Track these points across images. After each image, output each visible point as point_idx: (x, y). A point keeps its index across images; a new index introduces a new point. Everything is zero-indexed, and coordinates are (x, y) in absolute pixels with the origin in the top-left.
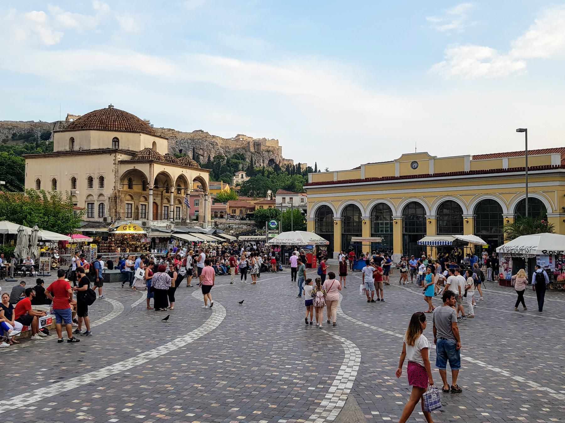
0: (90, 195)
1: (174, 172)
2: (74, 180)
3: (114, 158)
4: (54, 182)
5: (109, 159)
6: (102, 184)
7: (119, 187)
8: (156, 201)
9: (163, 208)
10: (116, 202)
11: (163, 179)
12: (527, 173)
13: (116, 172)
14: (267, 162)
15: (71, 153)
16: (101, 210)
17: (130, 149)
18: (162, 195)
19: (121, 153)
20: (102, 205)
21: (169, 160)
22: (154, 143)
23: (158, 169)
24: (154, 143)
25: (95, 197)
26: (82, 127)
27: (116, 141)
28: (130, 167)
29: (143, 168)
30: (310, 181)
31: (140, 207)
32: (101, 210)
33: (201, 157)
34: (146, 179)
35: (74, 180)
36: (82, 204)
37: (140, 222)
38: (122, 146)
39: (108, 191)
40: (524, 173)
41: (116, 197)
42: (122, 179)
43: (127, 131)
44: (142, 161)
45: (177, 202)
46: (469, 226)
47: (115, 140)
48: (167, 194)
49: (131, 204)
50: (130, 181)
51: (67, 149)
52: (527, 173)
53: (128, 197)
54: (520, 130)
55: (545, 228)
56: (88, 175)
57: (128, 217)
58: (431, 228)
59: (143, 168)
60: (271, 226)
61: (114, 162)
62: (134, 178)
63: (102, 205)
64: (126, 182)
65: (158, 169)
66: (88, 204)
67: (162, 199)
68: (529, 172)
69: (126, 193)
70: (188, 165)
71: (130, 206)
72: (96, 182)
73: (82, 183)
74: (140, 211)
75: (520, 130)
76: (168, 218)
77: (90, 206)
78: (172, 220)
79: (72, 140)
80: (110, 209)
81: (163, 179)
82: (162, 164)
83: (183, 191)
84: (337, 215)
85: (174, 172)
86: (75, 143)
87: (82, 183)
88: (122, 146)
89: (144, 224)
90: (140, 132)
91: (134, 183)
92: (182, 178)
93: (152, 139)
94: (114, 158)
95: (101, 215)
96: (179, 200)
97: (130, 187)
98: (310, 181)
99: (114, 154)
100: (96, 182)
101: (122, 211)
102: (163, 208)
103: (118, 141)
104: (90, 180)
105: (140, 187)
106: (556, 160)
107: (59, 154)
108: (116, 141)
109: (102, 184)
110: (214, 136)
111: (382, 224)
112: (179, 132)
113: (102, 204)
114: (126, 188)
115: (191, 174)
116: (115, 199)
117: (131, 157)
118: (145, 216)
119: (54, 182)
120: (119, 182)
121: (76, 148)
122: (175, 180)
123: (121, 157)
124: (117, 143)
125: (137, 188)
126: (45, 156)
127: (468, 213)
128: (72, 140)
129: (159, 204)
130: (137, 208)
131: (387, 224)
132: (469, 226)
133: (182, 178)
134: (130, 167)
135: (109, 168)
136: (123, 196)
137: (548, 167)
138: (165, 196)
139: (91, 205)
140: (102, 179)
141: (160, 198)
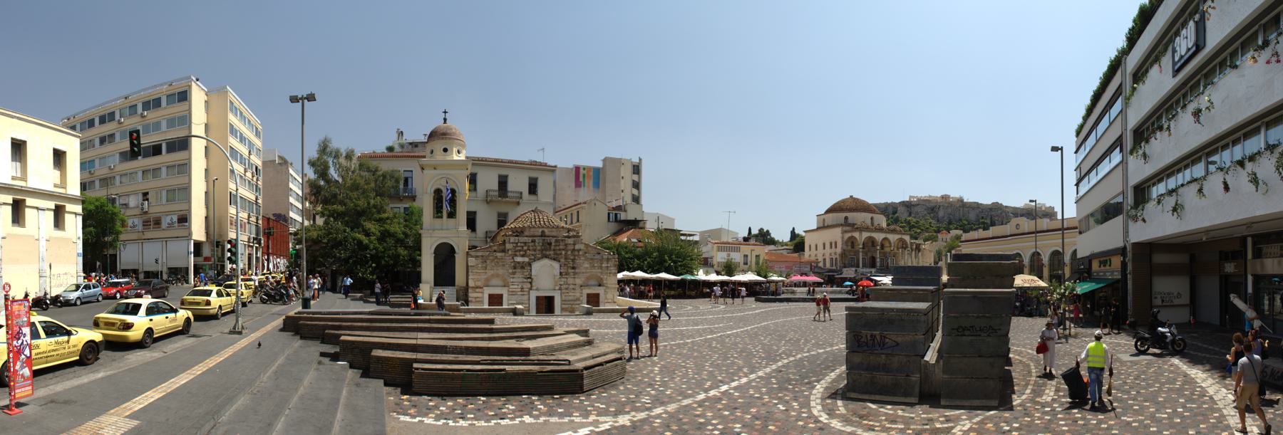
1: (879, 237)
5: (838, 231)
11: (872, 242)
21: (880, 230)
23: (865, 235)
27: (846, 218)
29: (856, 235)
36: (820, 259)
38: (850, 221)
39: (839, 250)
59: (856, 235)
62: (852, 242)
65: (865, 235)
87: (828, 245)
93: (870, 215)
108: (846, 218)
116: (843, 255)
133: (885, 239)
135: (836, 235)
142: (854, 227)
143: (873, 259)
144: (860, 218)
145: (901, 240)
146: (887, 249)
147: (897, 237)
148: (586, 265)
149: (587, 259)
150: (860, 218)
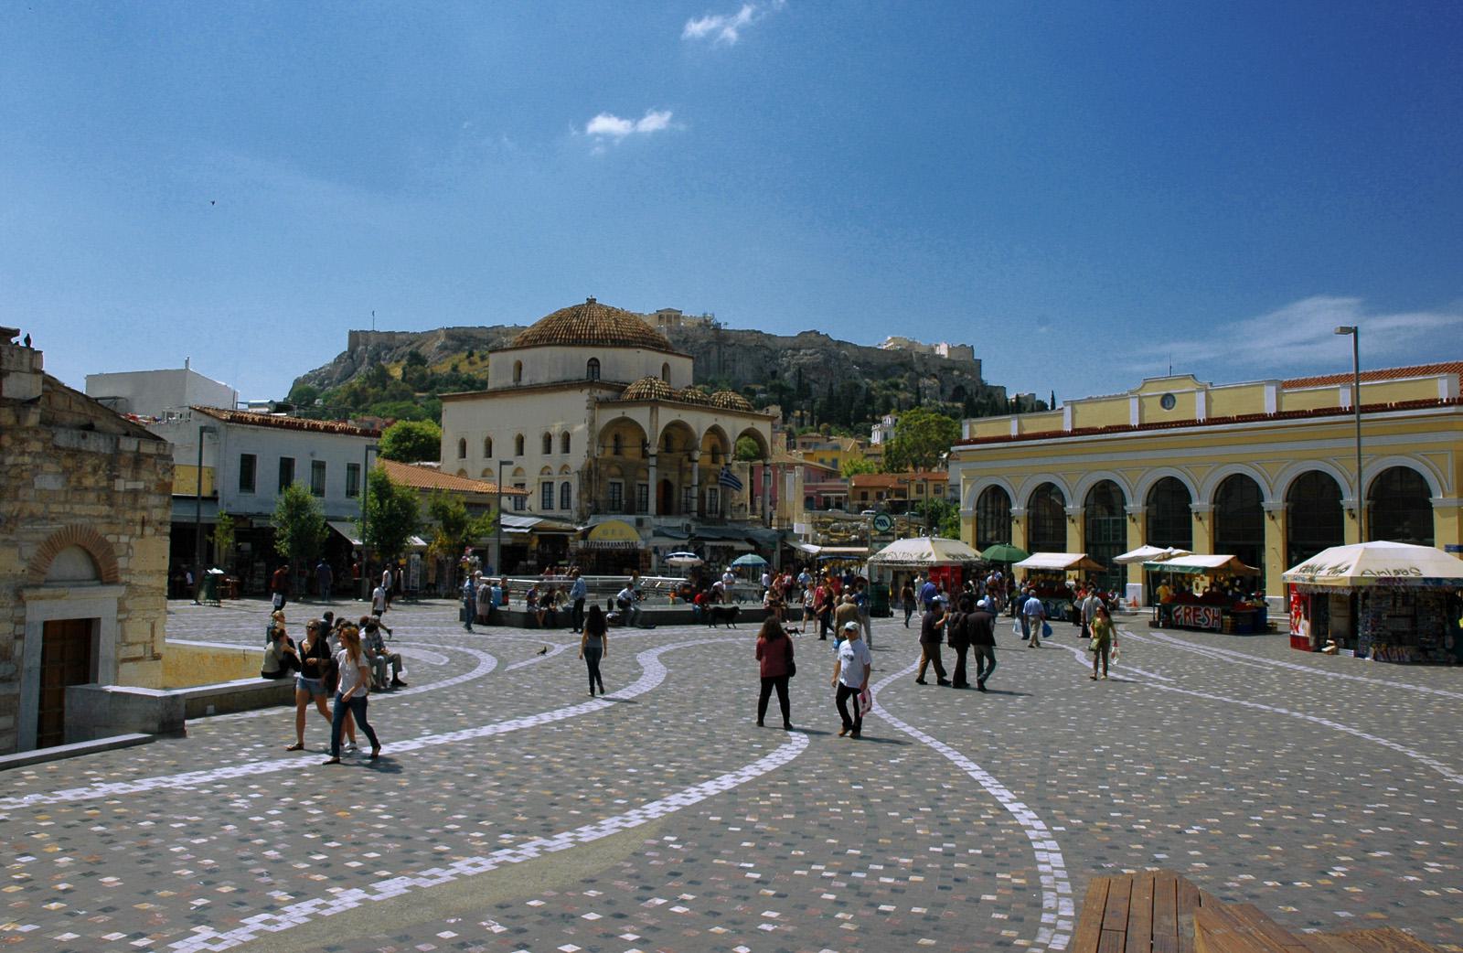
0: (547, 467)
1: (699, 422)
2: (520, 442)
3: (587, 397)
4: (489, 445)
5: (578, 400)
6: (566, 448)
7: (597, 452)
8: (670, 478)
9: (684, 491)
10: (590, 480)
11: (676, 436)
12: (1358, 417)
13: (592, 422)
14: (949, 392)
15: (517, 390)
16: (565, 496)
17: (622, 377)
18: (680, 465)
19: (598, 387)
20: (566, 487)
22: (666, 368)
23: (667, 416)
24: (666, 368)
25: (555, 470)
26: (536, 341)
27: (594, 363)
28: (615, 413)
29: (640, 415)
30: (966, 437)
31: (637, 490)
32: (565, 496)
33: (814, 386)
34: (645, 434)
35: (520, 442)
37: (632, 518)
39: (578, 458)
40: (1353, 417)
41: (590, 470)
42: (602, 436)
44: (639, 400)
45: (712, 478)
46: (1201, 531)
47: (593, 362)
48: (690, 465)
49: (620, 484)
50: (617, 438)
51: (510, 382)
52: (1358, 417)
53: (614, 470)
54: (1345, 331)
55: (1423, 535)
56: (543, 431)
57: (613, 509)
58: (1134, 531)
59: (640, 415)
60: (878, 527)
61: (586, 404)
63: (566, 487)
64: (610, 442)
65: (667, 416)
66: (544, 483)
67: (680, 474)
68: (1364, 416)
69: (610, 463)
70: (730, 409)
71: (617, 487)
72: (556, 444)
73: (534, 444)
74: (637, 496)
75: (1345, 331)
76: (688, 511)
77: (547, 487)
78: (695, 514)
79: (519, 366)
80: (580, 494)
81: (676, 436)
82: (674, 406)
83: (722, 458)
84: (1018, 508)
85: (699, 422)
86: (523, 371)
87: (534, 444)
88: (606, 373)
89: (639, 523)
90: (636, 347)
91: (627, 443)
92: (715, 430)
93: (659, 358)
94: (587, 397)
95: (565, 504)
96: (717, 477)
97: (617, 452)
98: (966, 437)
99: (587, 391)
100: (556, 444)
101: (601, 497)
102: (684, 491)
103: (598, 366)
104: (548, 440)
105: (638, 450)
106: (1442, 387)
107: (496, 393)
108: (594, 363)
109: (566, 448)
110: (840, 343)
111: (1106, 522)
112: (769, 337)
113: (567, 483)
114: (609, 453)
115: (733, 426)
116: (590, 475)
117: (615, 393)
118: (644, 509)
119: (489, 445)
121: (525, 381)
122: (702, 436)
123: (605, 394)
124: (596, 368)
125: (632, 453)
126: (473, 397)
127: (1201, 503)
128: (519, 366)
129: (675, 482)
130: (631, 491)
131: (1115, 522)
132: (1201, 531)
133: (715, 430)
134: (615, 413)
136: (603, 468)
137: (1432, 403)
138: (686, 468)
139: (547, 487)
140: (566, 438)
141: (676, 473)
142: (617, 392)
144: (633, 365)
145: (749, 433)
147: (744, 424)
148: (49, 480)
149: (54, 451)
150: (633, 365)
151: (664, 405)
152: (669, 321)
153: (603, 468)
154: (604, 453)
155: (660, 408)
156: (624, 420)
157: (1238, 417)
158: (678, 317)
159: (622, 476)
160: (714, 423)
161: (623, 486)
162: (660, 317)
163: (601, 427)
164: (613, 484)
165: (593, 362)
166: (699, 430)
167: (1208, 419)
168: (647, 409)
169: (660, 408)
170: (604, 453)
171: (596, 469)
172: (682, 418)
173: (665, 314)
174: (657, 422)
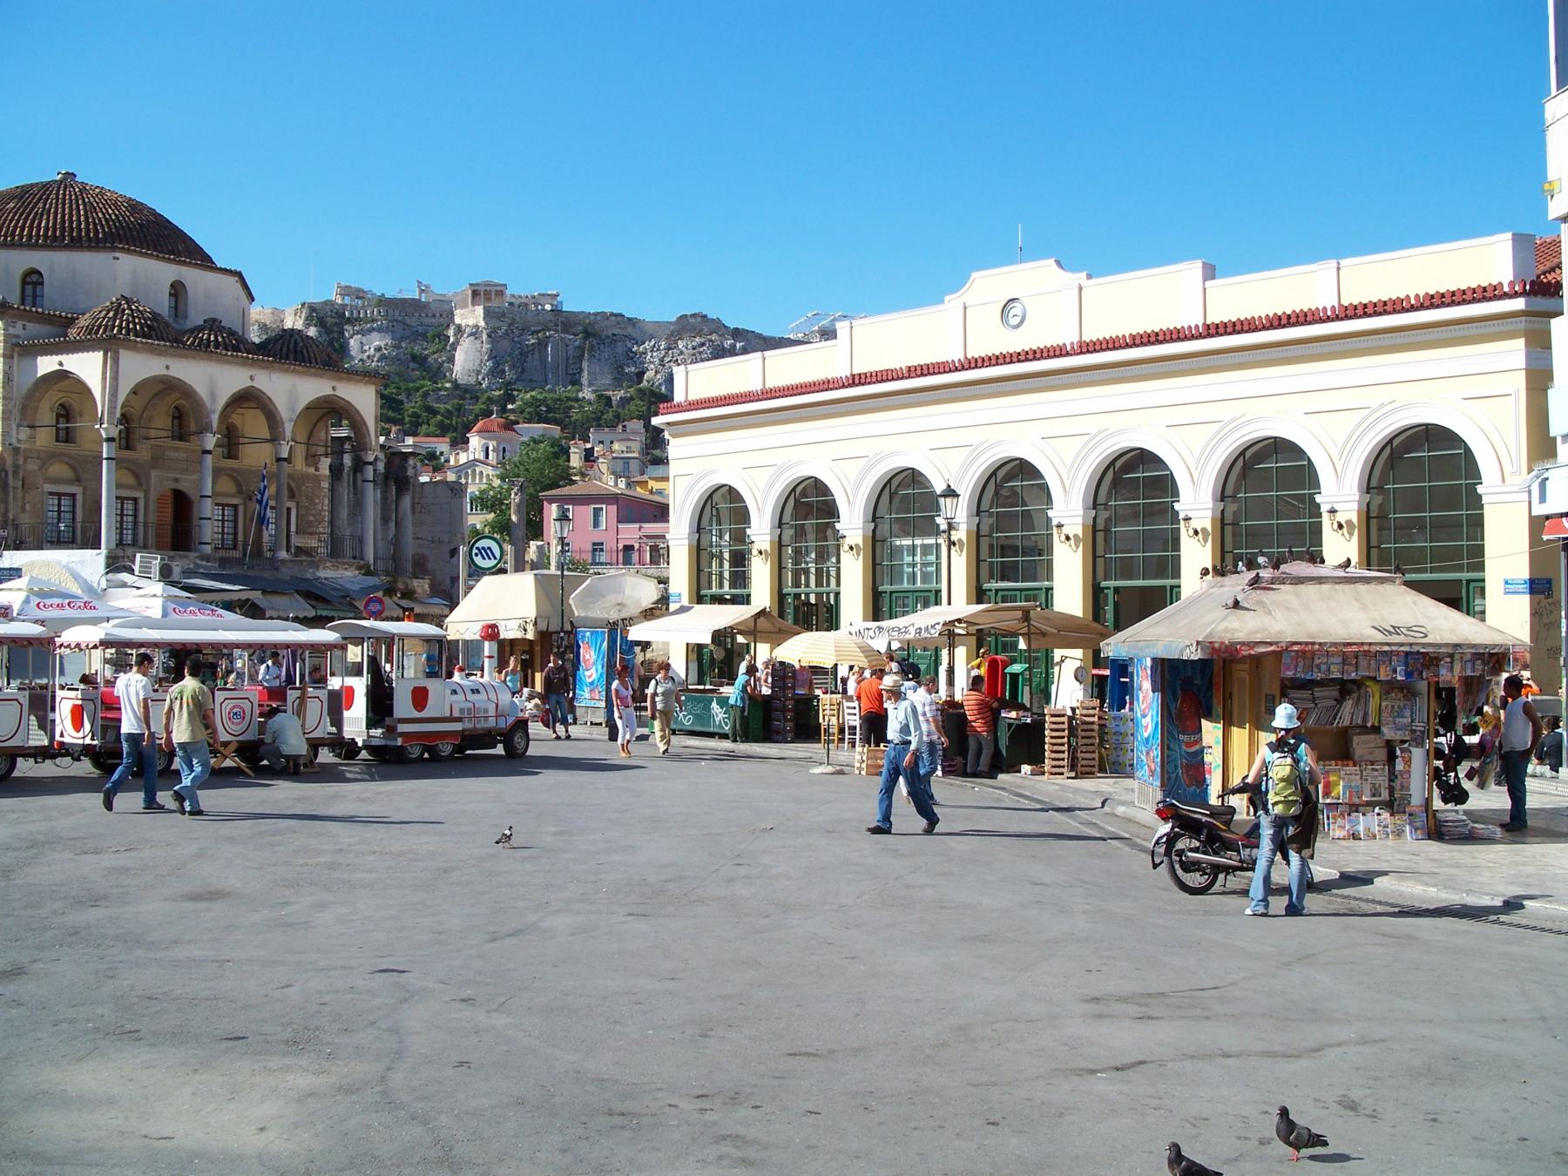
1: (214, 381)
19: (21, 318)
22: (177, 290)
24: (177, 290)
27: (32, 280)
29: (88, 367)
43: (77, 244)
47: (34, 278)
49: (73, 495)
53: (59, 470)
59: (88, 367)
60: (478, 560)
64: (46, 415)
69: (46, 458)
78: (208, 549)
85: (214, 381)
90: (114, 249)
108: (32, 280)
114: (45, 438)
120: (17, 415)
133: (247, 398)
136: (33, 466)
143: (182, 504)
146: (256, 456)
151: (133, 347)
152: (488, 299)
153: (33, 466)
154: (32, 438)
155: (122, 352)
156: (62, 375)
157: (1133, 337)
158: (501, 293)
159: (78, 480)
160: (250, 383)
161: (79, 498)
162: (475, 294)
163: (24, 390)
164: (59, 495)
165: (34, 278)
166: (213, 395)
167: (1081, 344)
168: (98, 356)
169: (122, 352)
170: (32, 438)
171: (16, 467)
172: (173, 373)
173: (482, 289)
174: (115, 378)
